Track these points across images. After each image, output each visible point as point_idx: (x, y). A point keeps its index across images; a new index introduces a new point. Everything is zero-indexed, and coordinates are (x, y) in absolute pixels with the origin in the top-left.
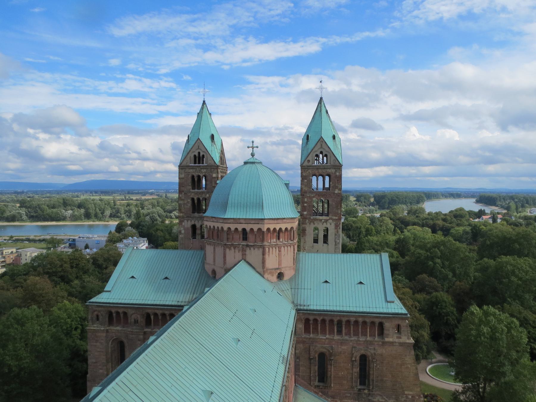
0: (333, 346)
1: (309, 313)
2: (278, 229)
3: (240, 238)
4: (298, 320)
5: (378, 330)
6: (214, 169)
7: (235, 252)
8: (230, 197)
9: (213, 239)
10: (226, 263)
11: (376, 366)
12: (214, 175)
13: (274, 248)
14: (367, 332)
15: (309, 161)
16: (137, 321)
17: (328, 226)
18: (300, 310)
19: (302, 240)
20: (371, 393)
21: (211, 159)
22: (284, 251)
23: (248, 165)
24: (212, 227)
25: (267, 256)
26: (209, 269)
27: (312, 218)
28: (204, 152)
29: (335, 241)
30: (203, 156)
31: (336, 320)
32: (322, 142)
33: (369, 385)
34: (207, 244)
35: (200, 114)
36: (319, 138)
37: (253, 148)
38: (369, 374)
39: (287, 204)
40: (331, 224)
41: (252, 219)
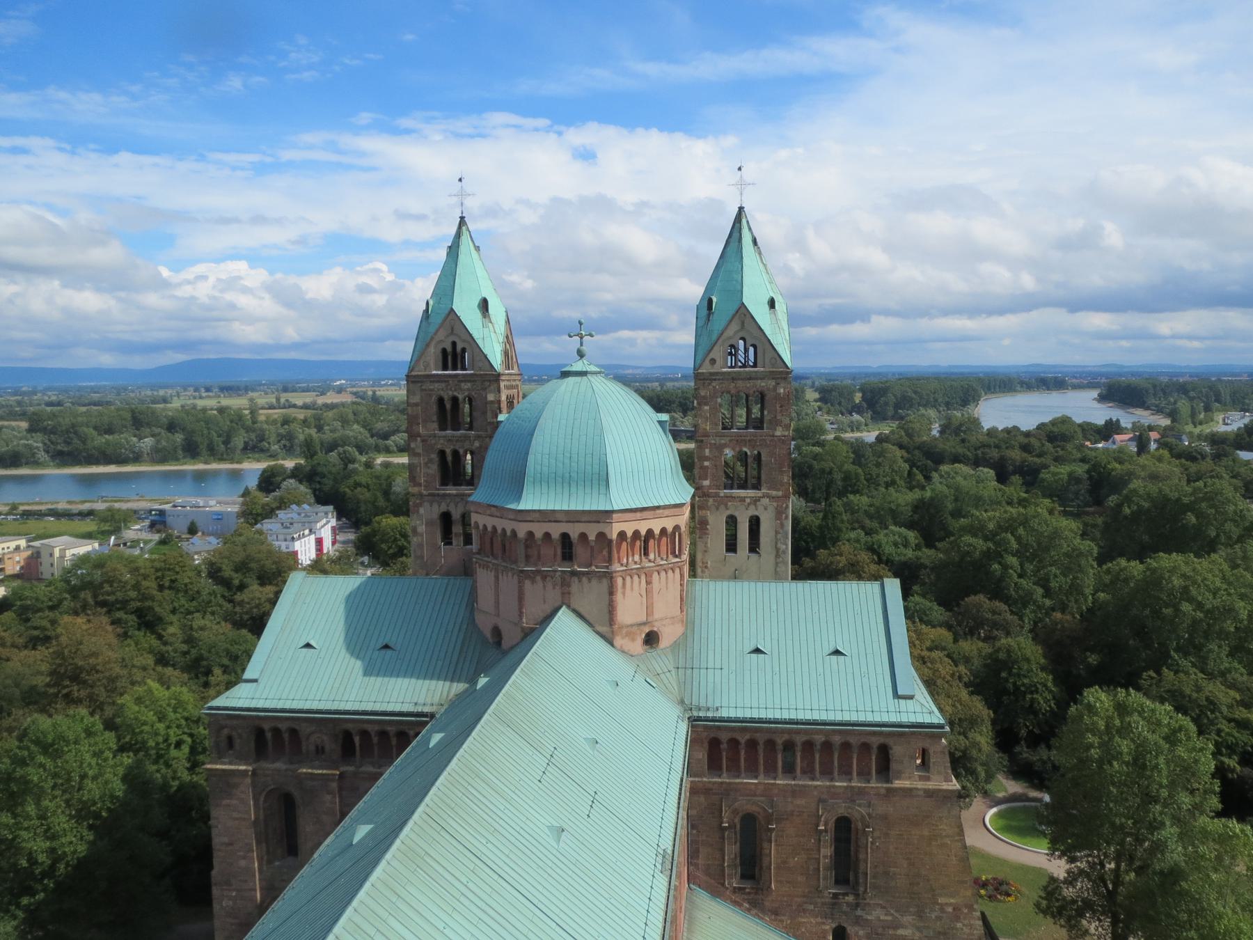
0: (775, 799)
1: (719, 728)
2: (643, 533)
3: (555, 555)
5: (876, 762)
7: (544, 587)
8: (531, 458)
9: (492, 554)
12: (491, 397)
13: (636, 578)
14: (851, 766)
15: (713, 361)
16: (323, 748)
18: (699, 719)
19: (700, 546)
20: (861, 901)
22: (660, 582)
23: (571, 380)
24: (489, 529)
25: (619, 597)
26: (485, 624)
27: (722, 495)
28: (464, 341)
30: (464, 350)
31: (780, 741)
33: (857, 883)
34: (480, 566)
36: (736, 307)
37: (581, 338)
39: (663, 472)
40: (766, 509)
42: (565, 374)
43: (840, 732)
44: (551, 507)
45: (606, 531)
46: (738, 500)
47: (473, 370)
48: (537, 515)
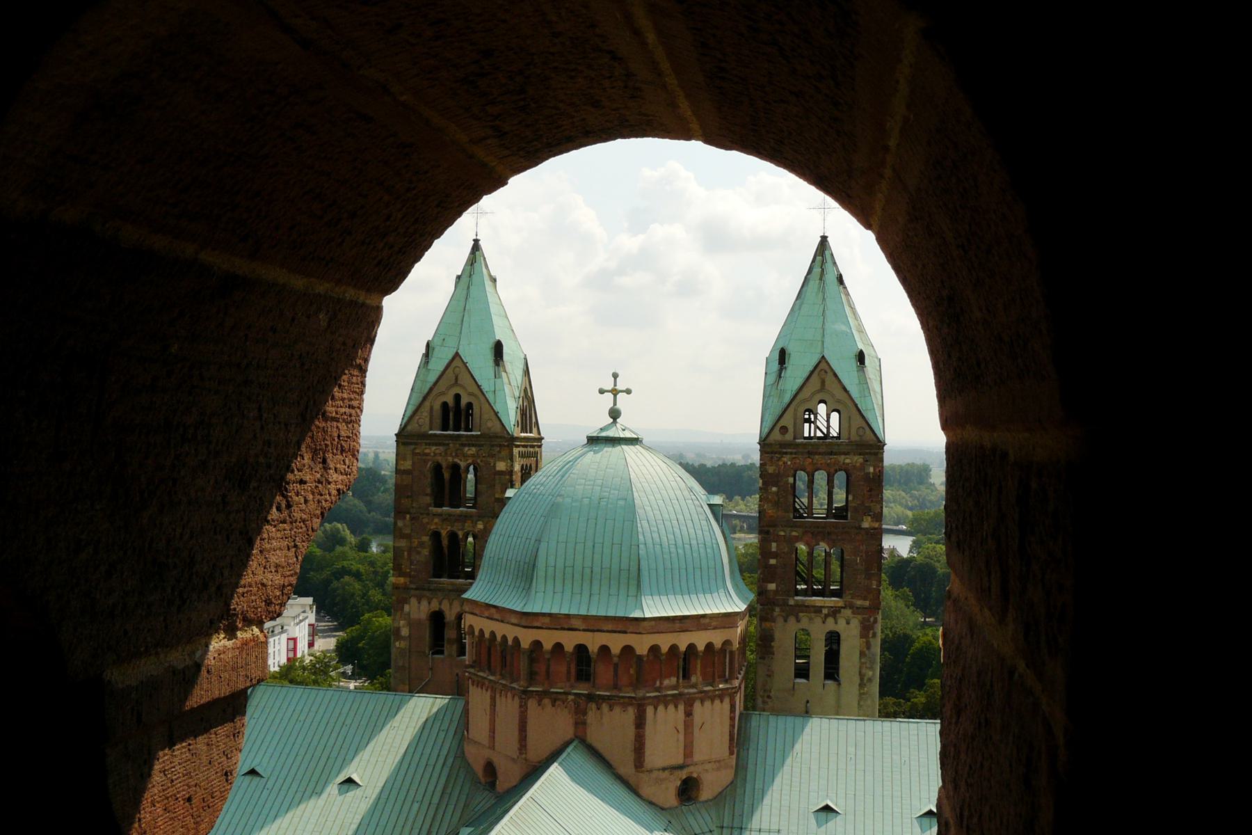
2: (683, 648)
3: (569, 672)
6: (500, 446)
9: (489, 670)
10: (525, 746)
12: (501, 466)
15: (784, 430)
17: (841, 626)
21: (494, 417)
24: (487, 635)
26: (477, 757)
27: (791, 602)
29: (860, 672)
30: (470, 405)
34: (473, 682)
35: (465, 279)
37: (615, 396)
39: (712, 571)
40: (848, 623)
41: (607, 618)
46: (812, 609)
47: (480, 431)
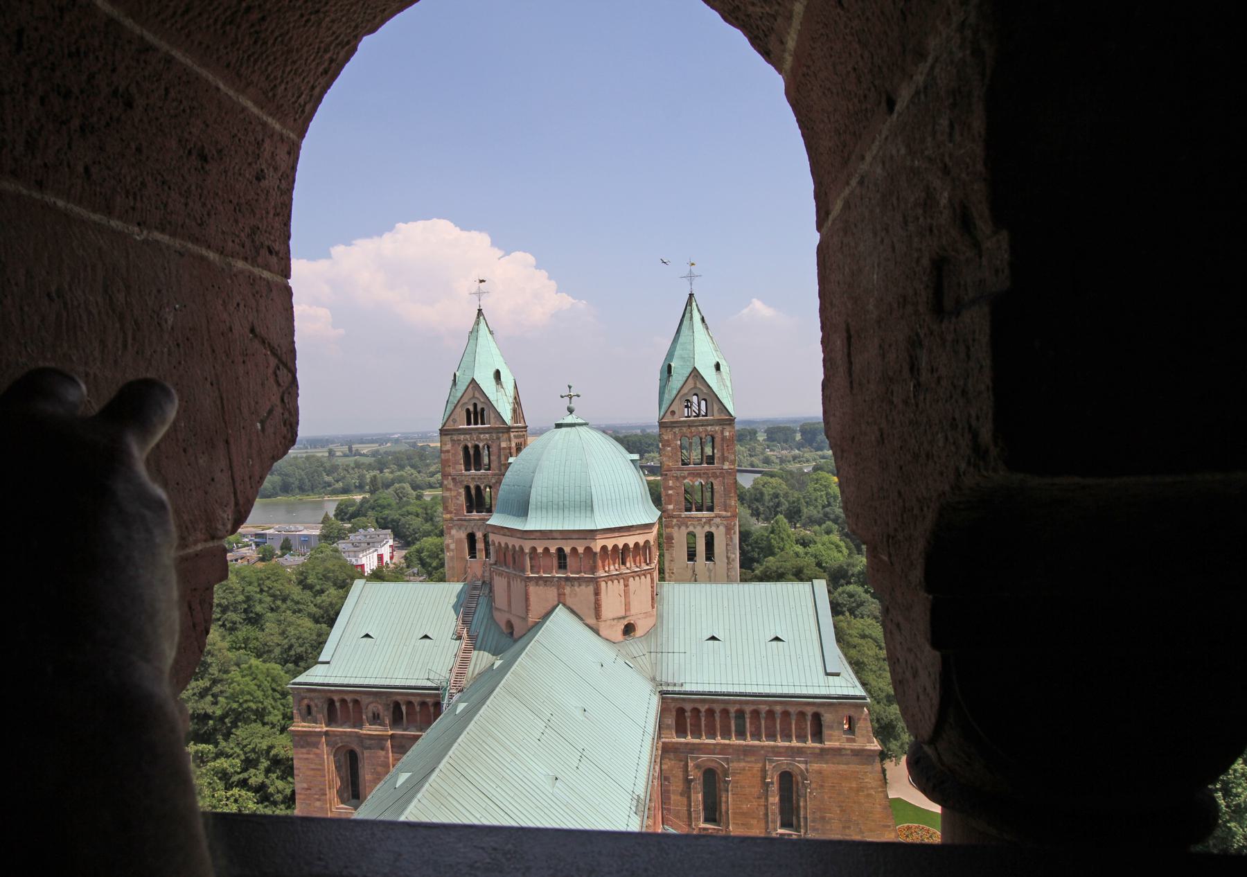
1: (683, 699)
2: (621, 547)
4: (663, 711)
8: (533, 491)
9: (506, 565)
11: (810, 793)
12: (503, 445)
13: (616, 581)
14: (791, 730)
15: (673, 413)
17: (713, 530)
18: (668, 693)
19: (667, 556)
23: (564, 429)
24: (503, 545)
26: (501, 619)
27: (683, 516)
30: (483, 410)
31: (732, 709)
32: (697, 376)
35: (474, 334)
36: (690, 370)
37: (570, 398)
38: (798, 807)
39: (635, 499)
42: (559, 426)
43: (781, 703)
44: (549, 528)
45: (592, 546)
48: (538, 534)
